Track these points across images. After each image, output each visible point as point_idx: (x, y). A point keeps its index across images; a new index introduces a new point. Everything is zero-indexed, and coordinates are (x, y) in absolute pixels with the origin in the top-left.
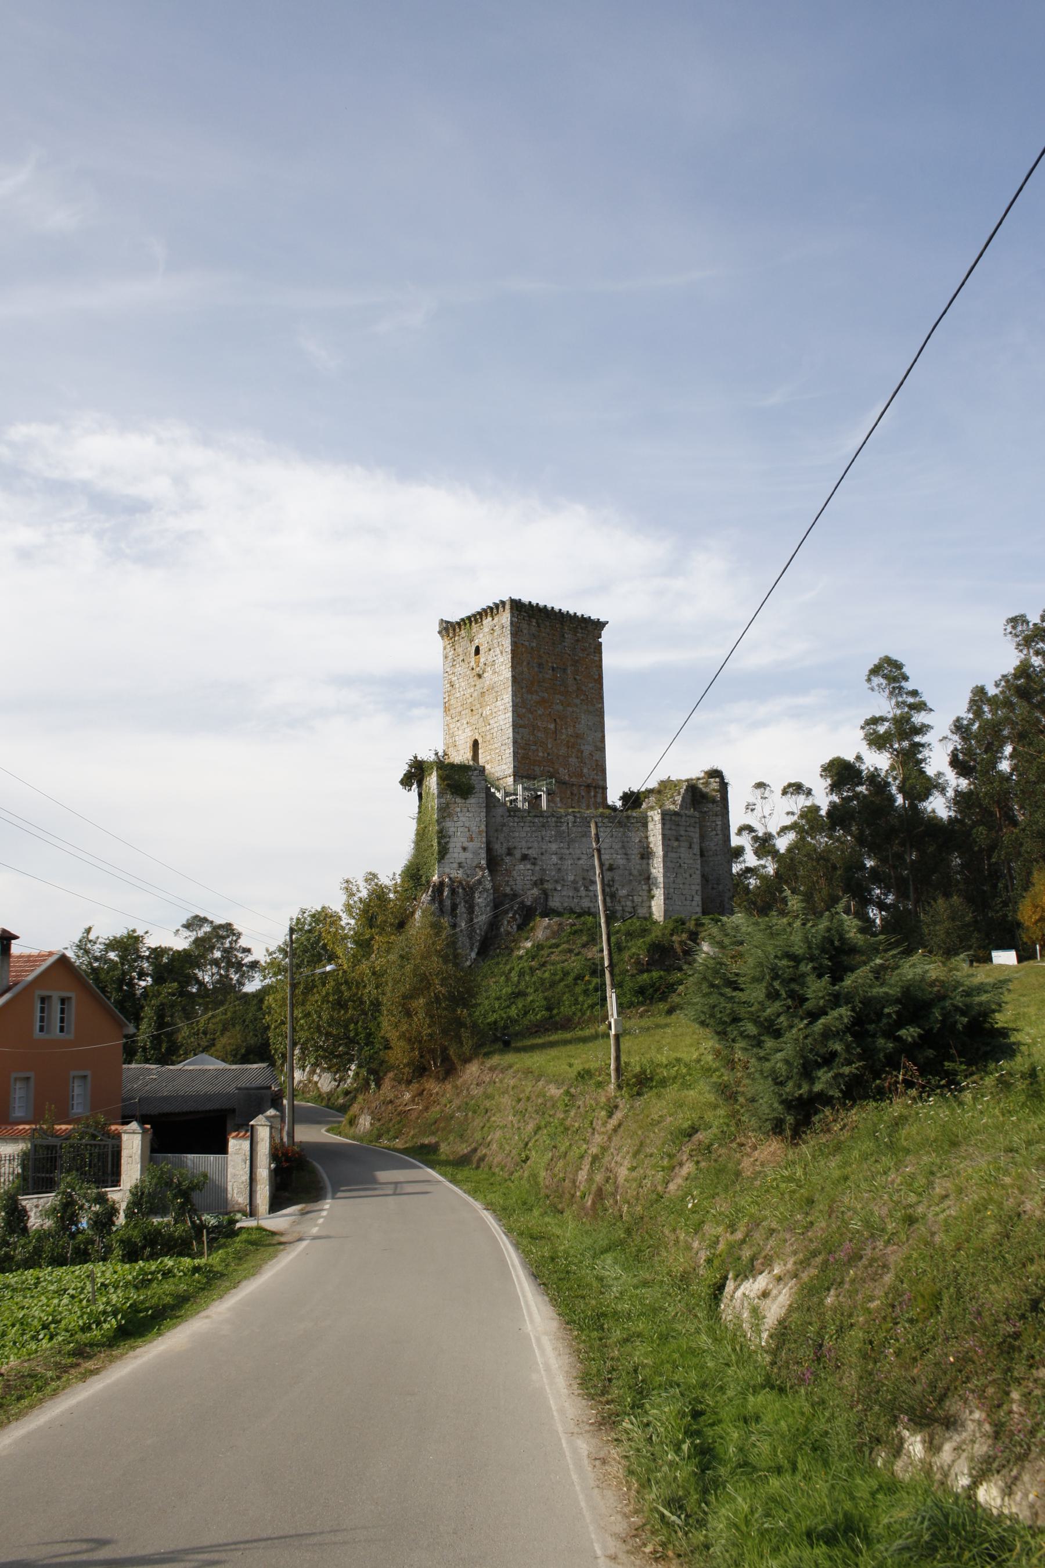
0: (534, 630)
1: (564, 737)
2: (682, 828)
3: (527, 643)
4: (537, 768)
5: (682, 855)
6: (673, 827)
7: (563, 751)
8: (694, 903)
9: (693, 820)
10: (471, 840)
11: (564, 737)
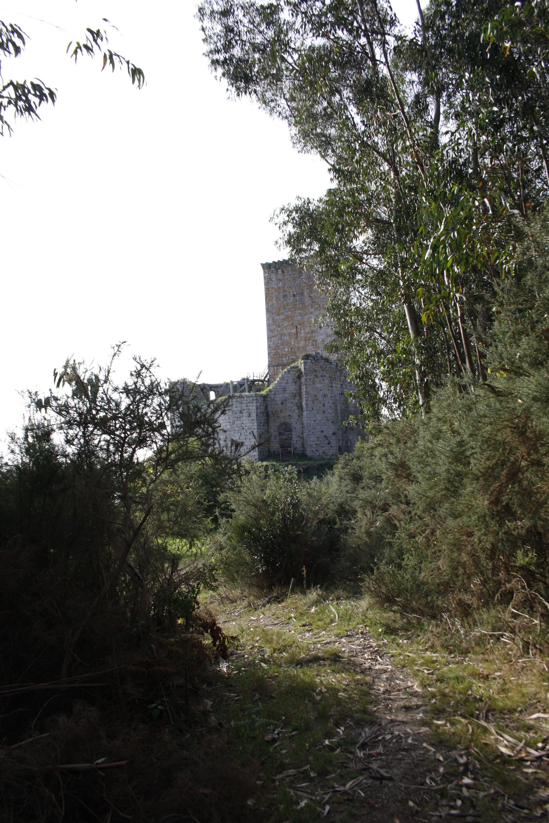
0: (280, 276)
1: (303, 335)
2: (244, 405)
3: (275, 286)
4: (284, 359)
5: (244, 422)
6: (238, 405)
7: (302, 343)
9: (251, 399)
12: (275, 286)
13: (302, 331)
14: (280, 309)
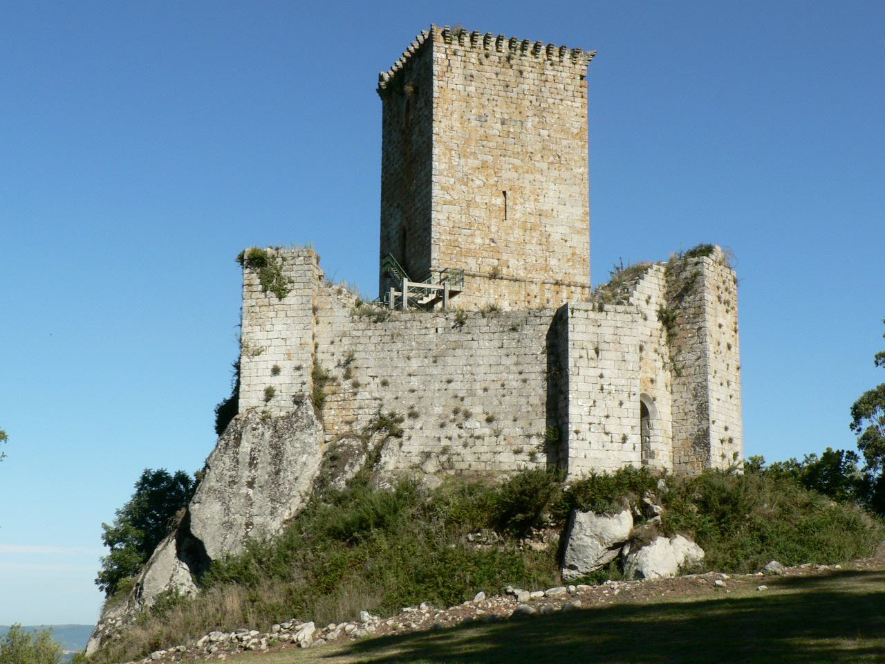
1: (518, 215)
5: (606, 373)
7: (517, 233)
8: (628, 445)
10: (289, 356)
11: (518, 215)
12: (460, 88)
13: (518, 207)
14: (467, 141)
